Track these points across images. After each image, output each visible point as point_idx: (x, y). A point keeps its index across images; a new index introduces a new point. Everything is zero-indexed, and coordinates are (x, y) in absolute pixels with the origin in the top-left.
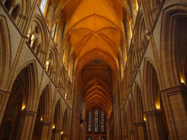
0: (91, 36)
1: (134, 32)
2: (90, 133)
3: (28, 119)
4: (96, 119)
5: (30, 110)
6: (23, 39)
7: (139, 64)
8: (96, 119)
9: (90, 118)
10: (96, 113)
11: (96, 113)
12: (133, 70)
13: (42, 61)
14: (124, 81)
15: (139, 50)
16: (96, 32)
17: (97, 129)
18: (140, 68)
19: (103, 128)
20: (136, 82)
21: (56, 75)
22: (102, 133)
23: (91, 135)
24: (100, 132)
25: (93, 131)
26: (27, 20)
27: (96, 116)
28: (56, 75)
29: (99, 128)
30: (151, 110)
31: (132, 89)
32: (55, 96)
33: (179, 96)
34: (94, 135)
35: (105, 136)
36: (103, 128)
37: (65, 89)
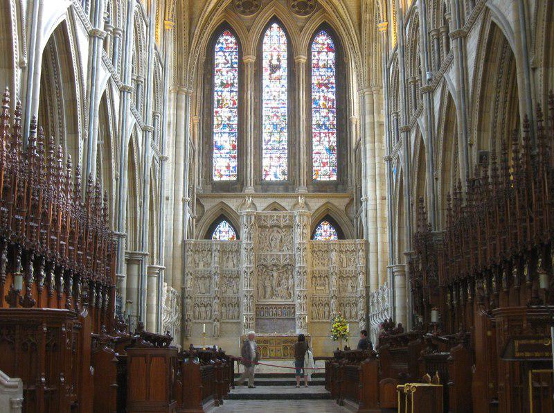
2: (226, 187)
4: (274, 90)
8: (274, 90)
9: (222, 85)
10: (274, 43)
11: (274, 43)
17: (284, 161)
19: (330, 150)
22: (322, 187)
23: (233, 204)
24: (303, 178)
25: (250, 173)
27: (274, 69)
29: (297, 151)
34: (261, 205)
35: (339, 203)
36: (330, 150)
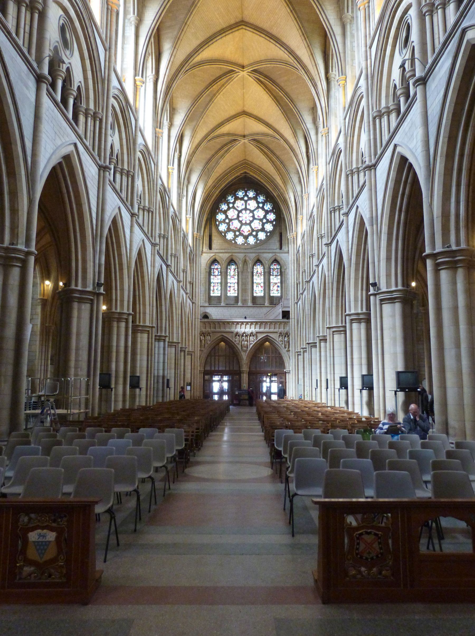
0: (231, 78)
1: (345, 119)
3: (118, 327)
5: (118, 311)
6: (102, 172)
7: (349, 206)
12: (336, 205)
13: (125, 196)
14: (315, 213)
15: (352, 173)
16: (243, 67)
18: (349, 216)
20: (339, 243)
21: (150, 214)
26: (101, 120)
28: (150, 214)
30: (360, 311)
31: (329, 251)
32: (153, 266)
33: (398, 306)
37: (167, 239)
